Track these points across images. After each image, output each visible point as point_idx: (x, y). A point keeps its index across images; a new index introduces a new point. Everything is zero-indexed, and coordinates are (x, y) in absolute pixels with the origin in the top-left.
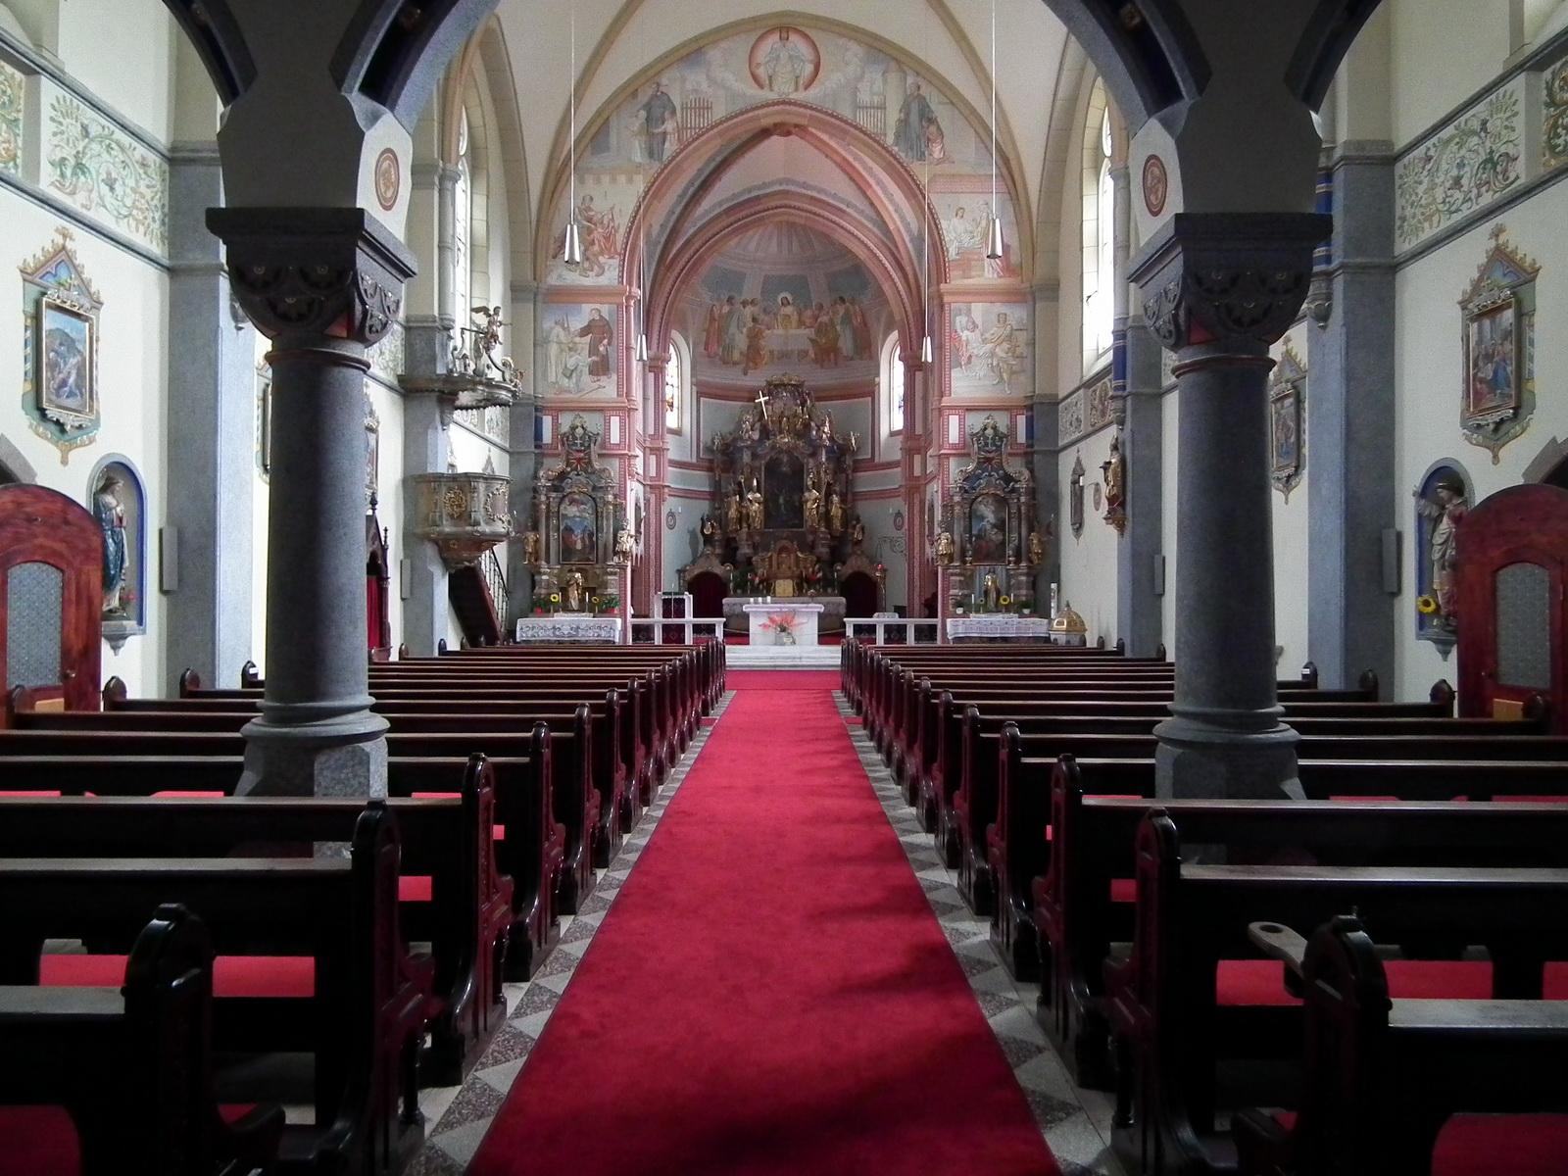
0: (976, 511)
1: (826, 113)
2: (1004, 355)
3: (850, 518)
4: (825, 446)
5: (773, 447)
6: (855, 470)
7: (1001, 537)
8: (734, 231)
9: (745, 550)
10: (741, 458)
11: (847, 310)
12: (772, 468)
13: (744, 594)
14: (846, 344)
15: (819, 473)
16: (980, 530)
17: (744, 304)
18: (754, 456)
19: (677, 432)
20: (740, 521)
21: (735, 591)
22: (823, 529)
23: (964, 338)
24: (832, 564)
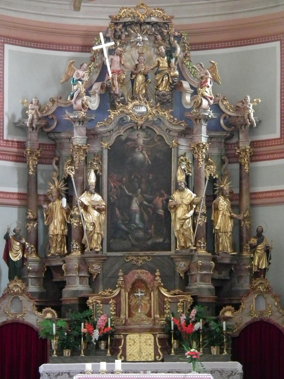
3: (246, 236)
4: (207, 119)
5: (122, 122)
6: (254, 157)
9: (76, 286)
12: (119, 154)
13: (75, 356)
18: (92, 135)
20: (68, 239)
21: (60, 353)
22: (202, 252)
24: (217, 308)
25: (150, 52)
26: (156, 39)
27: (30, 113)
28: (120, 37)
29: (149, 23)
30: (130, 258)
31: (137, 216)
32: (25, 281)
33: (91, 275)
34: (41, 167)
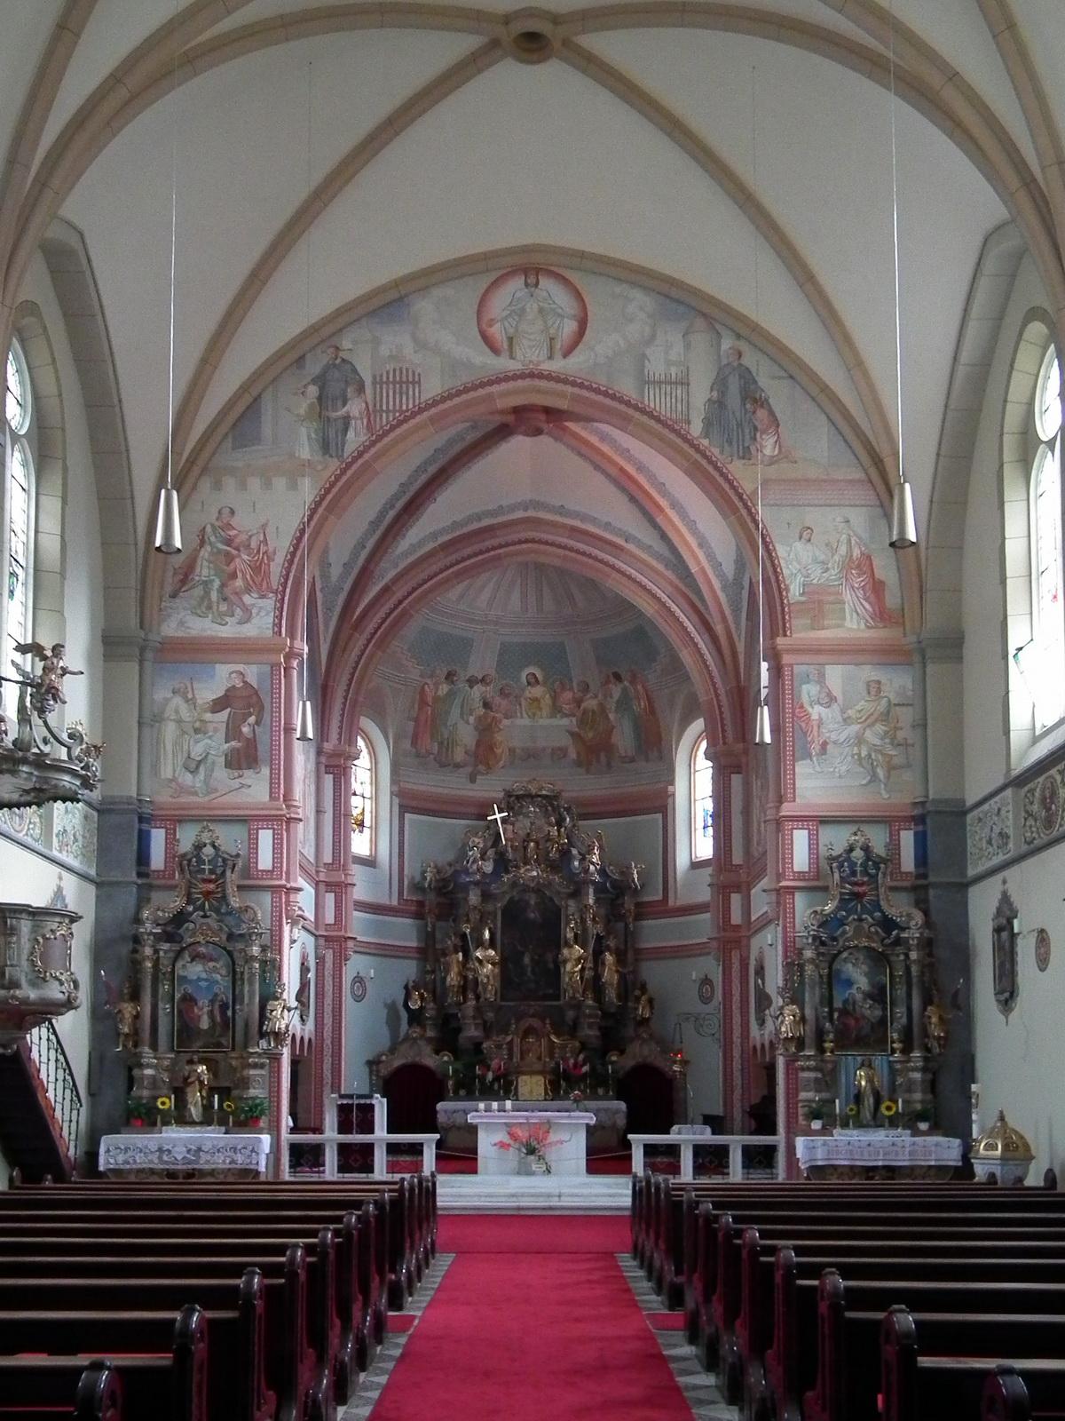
0: (839, 972)
1: (597, 391)
2: (878, 742)
3: (631, 987)
4: (593, 882)
5: (514, 884)
6: (639, 917)
7: (878, 1013)
8: (458, 575)
9: (472, 1031)
10: (466, 900)
11: (625, 690)
12: (513, 914)
13: (470, 1096)
14: (624, 739)
15: (583, 921)
16: (846, 1002)
17: (472, 682)
18: (486, 896)
19: (370, 862)
20: (463, 989)
21: (456, 1092)
22: (590, 1002)
23: (815, 717)
24: (604, 1053)
25: (541, 822)
26: (547, 810)
27: (429, 876)
28: (512, 808)
29: (540, 796)
30: (522, 1008)
31: (529, 969)
32: (423, 1027)
33: (485, 1022)
34: (439, 924)
